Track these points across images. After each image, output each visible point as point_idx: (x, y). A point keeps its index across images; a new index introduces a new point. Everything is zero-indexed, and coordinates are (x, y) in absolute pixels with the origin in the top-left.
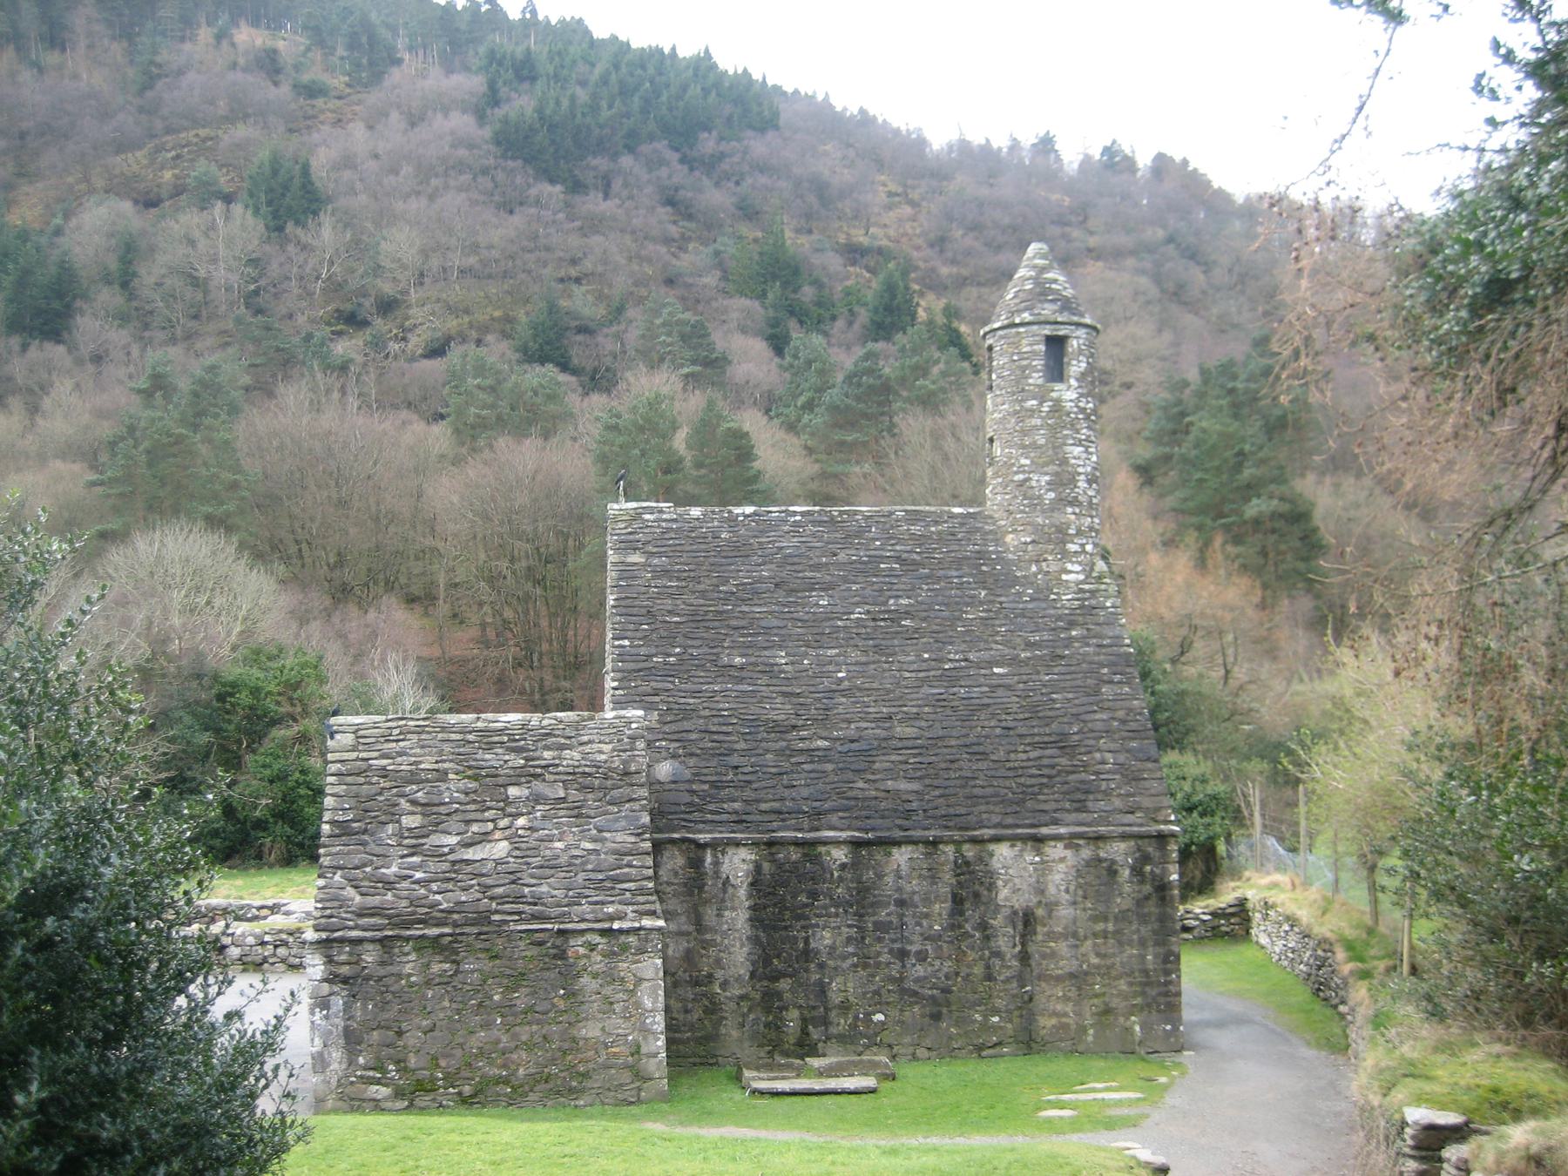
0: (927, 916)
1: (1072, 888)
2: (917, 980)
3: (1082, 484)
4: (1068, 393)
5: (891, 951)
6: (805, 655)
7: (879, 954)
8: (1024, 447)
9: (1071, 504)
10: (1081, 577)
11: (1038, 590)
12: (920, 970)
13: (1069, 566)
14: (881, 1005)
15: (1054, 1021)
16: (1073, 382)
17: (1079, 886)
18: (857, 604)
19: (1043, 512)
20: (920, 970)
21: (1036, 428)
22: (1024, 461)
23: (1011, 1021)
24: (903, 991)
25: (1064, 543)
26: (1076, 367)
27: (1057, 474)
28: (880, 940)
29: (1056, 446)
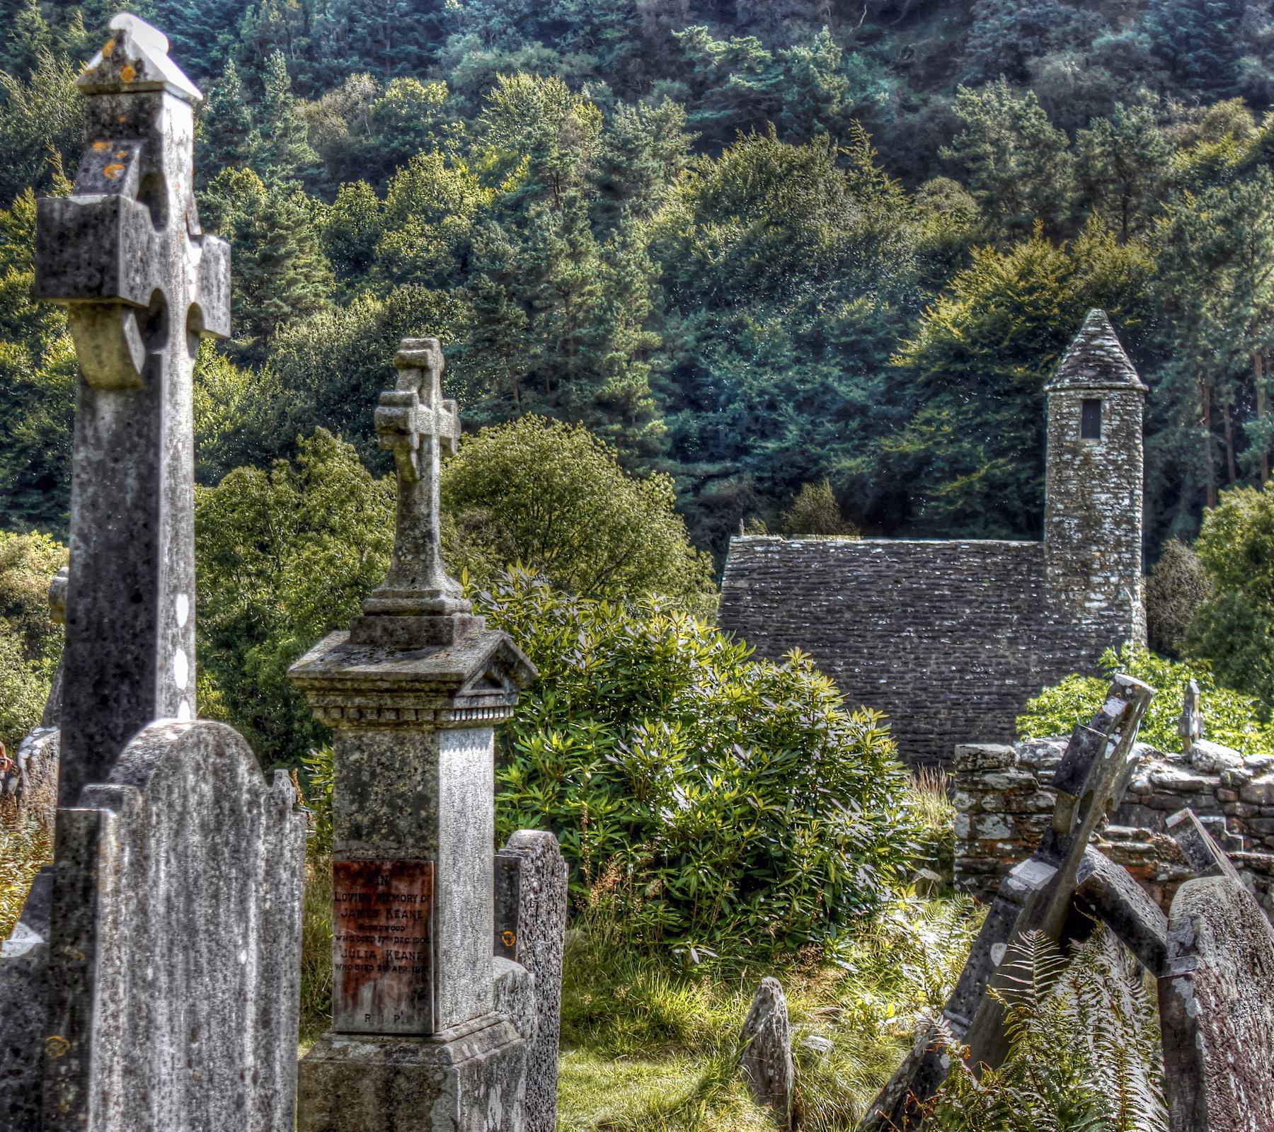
3: (1108, 524)
4: (1097, 449)
6: (856, 664)
8: (1060, 494)
9: (1096, 543)
10: (1104, 605)
11: (1064, 616)
13: (1093, 596)
16: (1104, 439)
18: (909, 624)
21: (1069, 478)
22: (1060, 506)
25: (1088, 575)
26: (1105, 427)
27: (1084, 518)
29: (1085, 494)
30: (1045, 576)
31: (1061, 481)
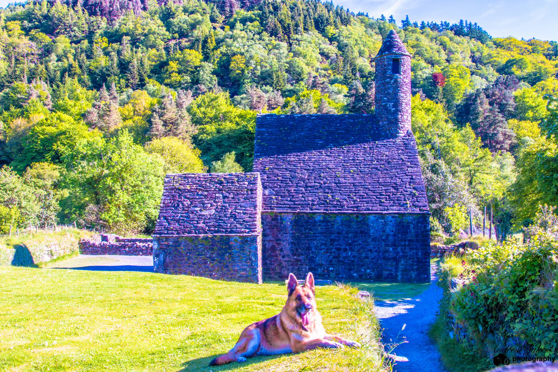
0: (347, 237)
1: (394, 230)
2: (344, 258)
5: (335, 248)
7: (332, 249)
12: (344, 254)
14: (332, 265)
15: (388, 272)
17: (396, 230)
19: (391, 114)
20: (344, 254)
22: (385, 99)
23: (374, 272)
24: (339, 261)
28: (332, 245)
30: (379, 125)
31: (385, 89)
